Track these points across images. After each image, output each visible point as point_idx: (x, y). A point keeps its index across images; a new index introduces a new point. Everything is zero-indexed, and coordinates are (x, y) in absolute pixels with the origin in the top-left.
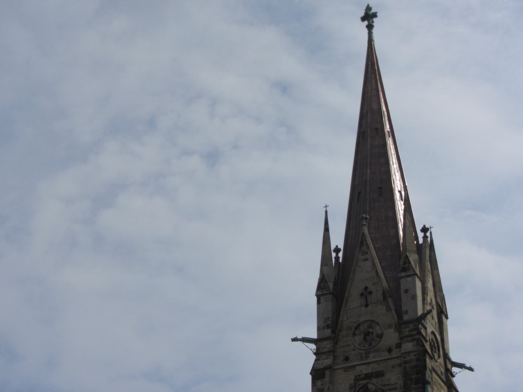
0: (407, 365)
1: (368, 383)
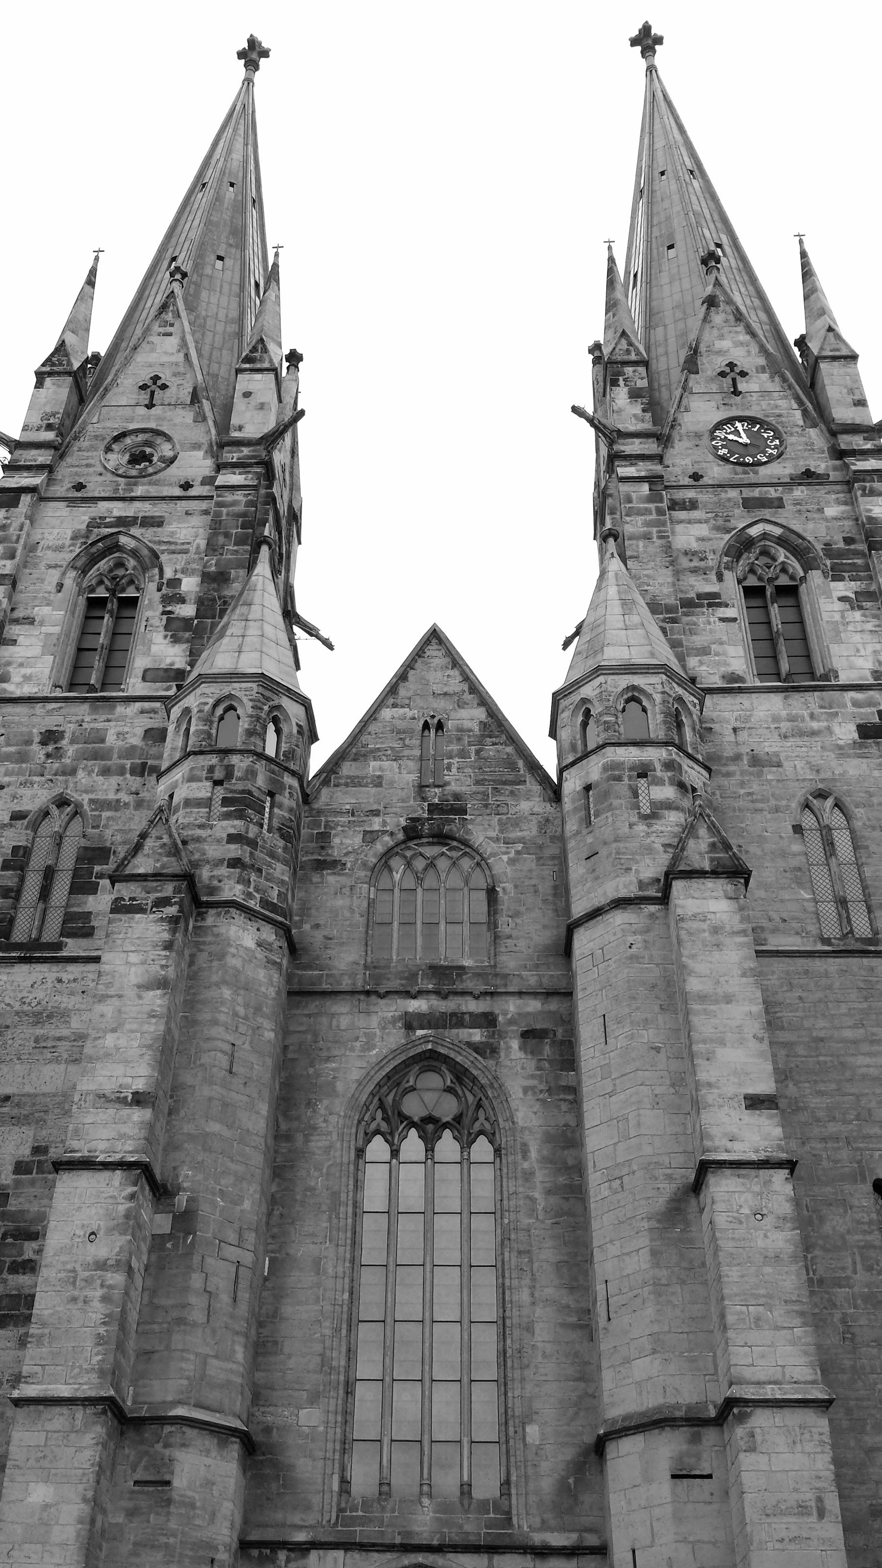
0: (224, 510)
1: (119, 533)
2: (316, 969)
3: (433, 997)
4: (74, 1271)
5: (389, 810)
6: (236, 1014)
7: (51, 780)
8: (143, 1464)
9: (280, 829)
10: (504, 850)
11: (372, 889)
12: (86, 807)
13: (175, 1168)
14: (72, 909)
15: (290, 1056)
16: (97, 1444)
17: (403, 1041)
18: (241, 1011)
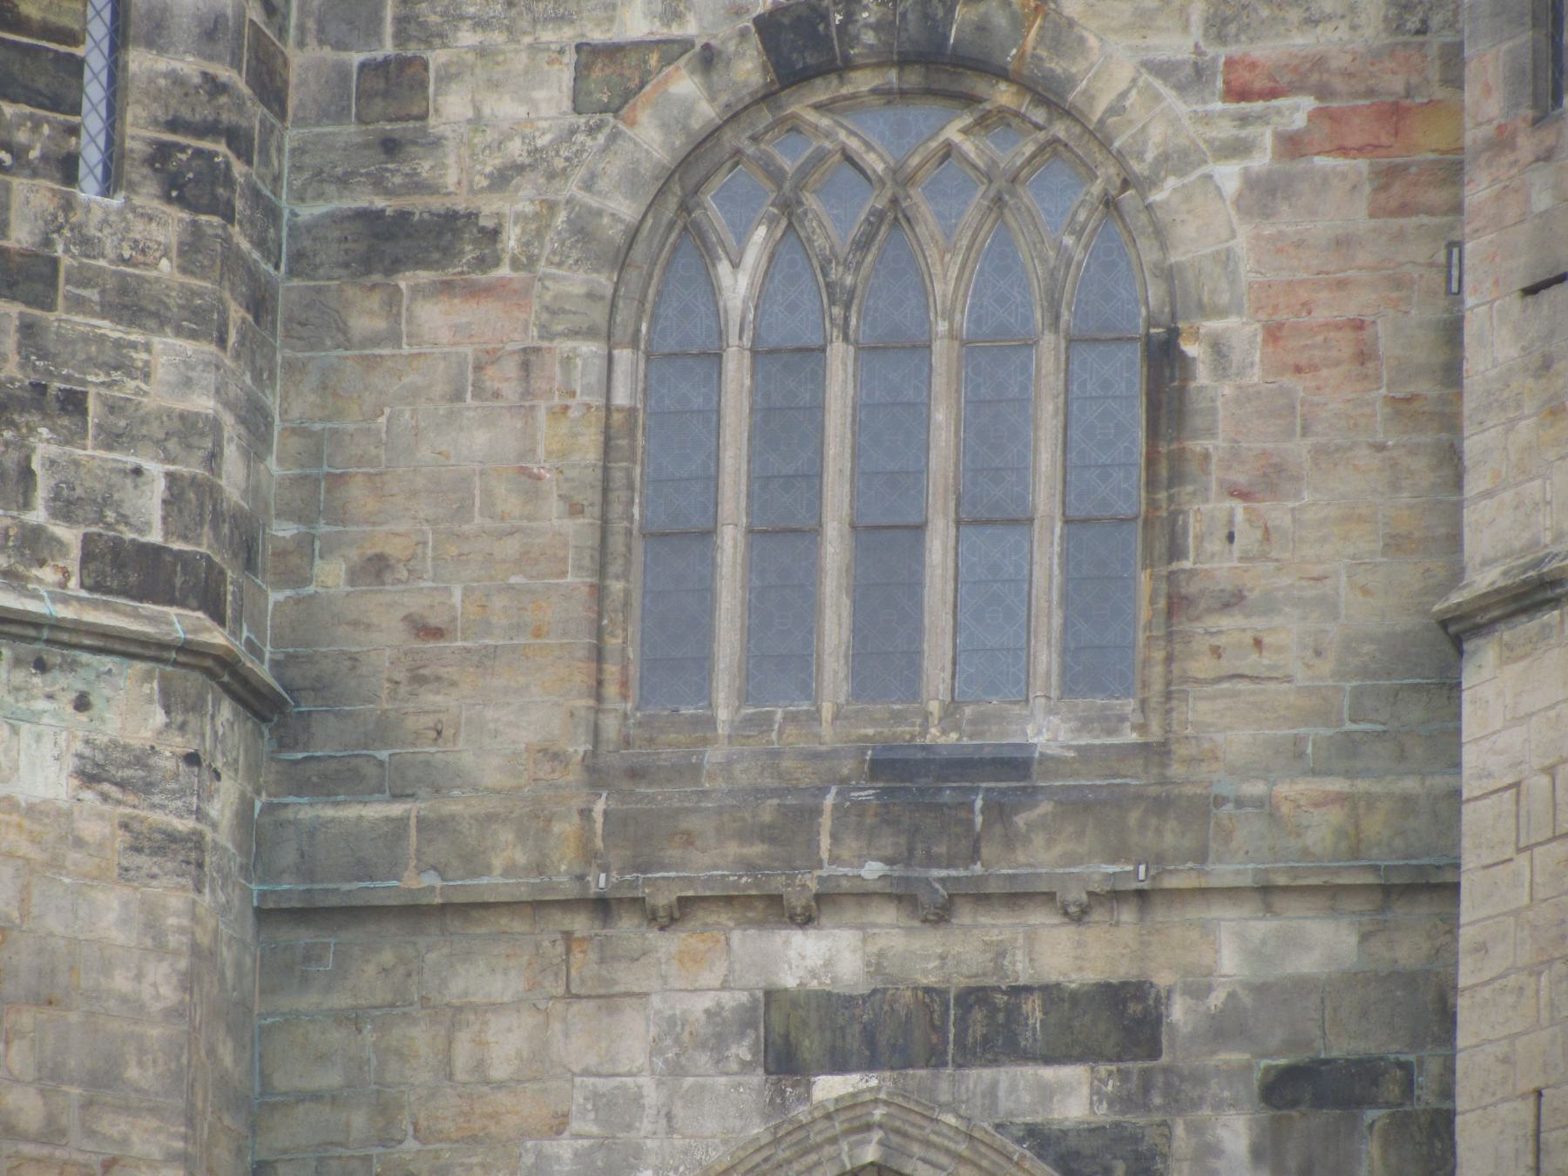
3: (887, 915)
9: (161, 154)
10: (1225, 130)
11: (623, 356)
17: (757, 1129)
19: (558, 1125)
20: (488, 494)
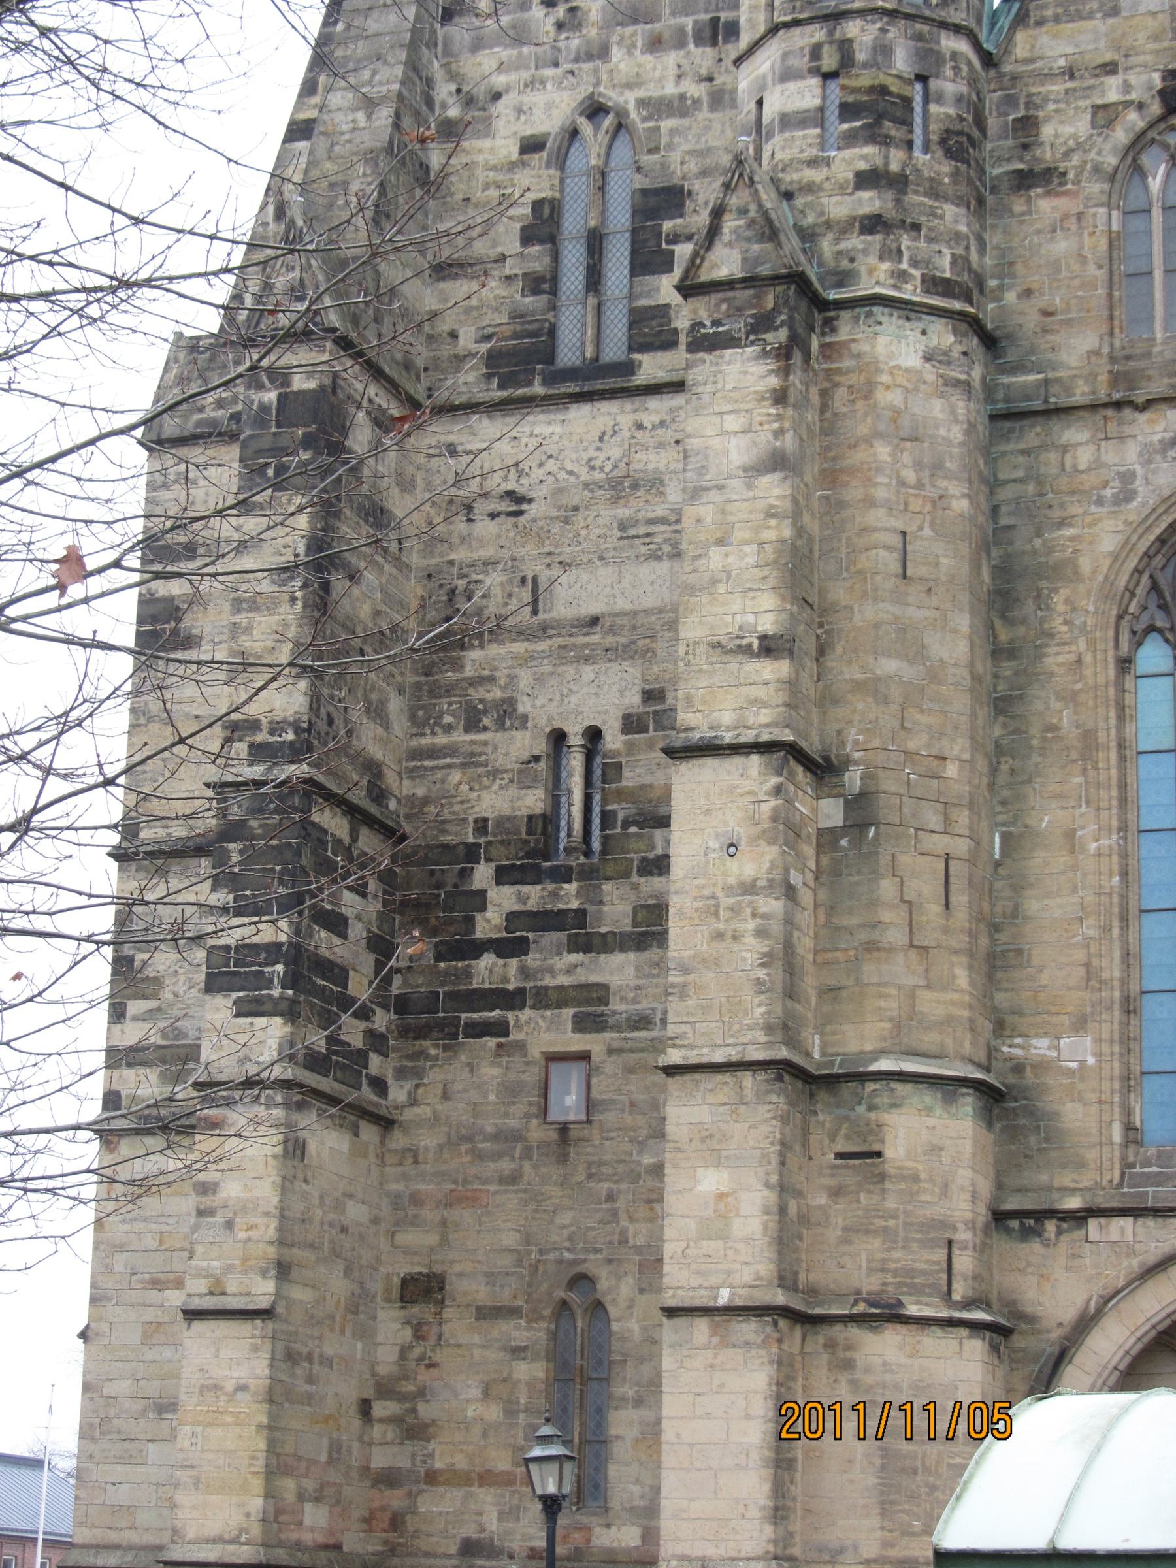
2: (1031, 371)
4: (714, 897)
5: (1133, 60)
6: (902, 483)
7: (572, 72)
8: (843, 1131)
11: (1115, 213)
12: (633, 115)
13: (839, 732)
14: (643, 302)
15: (1004, 521)
16: (774, 1118)
18: (910, 475)
19: (1105, 485)
20: (1068, 265)
